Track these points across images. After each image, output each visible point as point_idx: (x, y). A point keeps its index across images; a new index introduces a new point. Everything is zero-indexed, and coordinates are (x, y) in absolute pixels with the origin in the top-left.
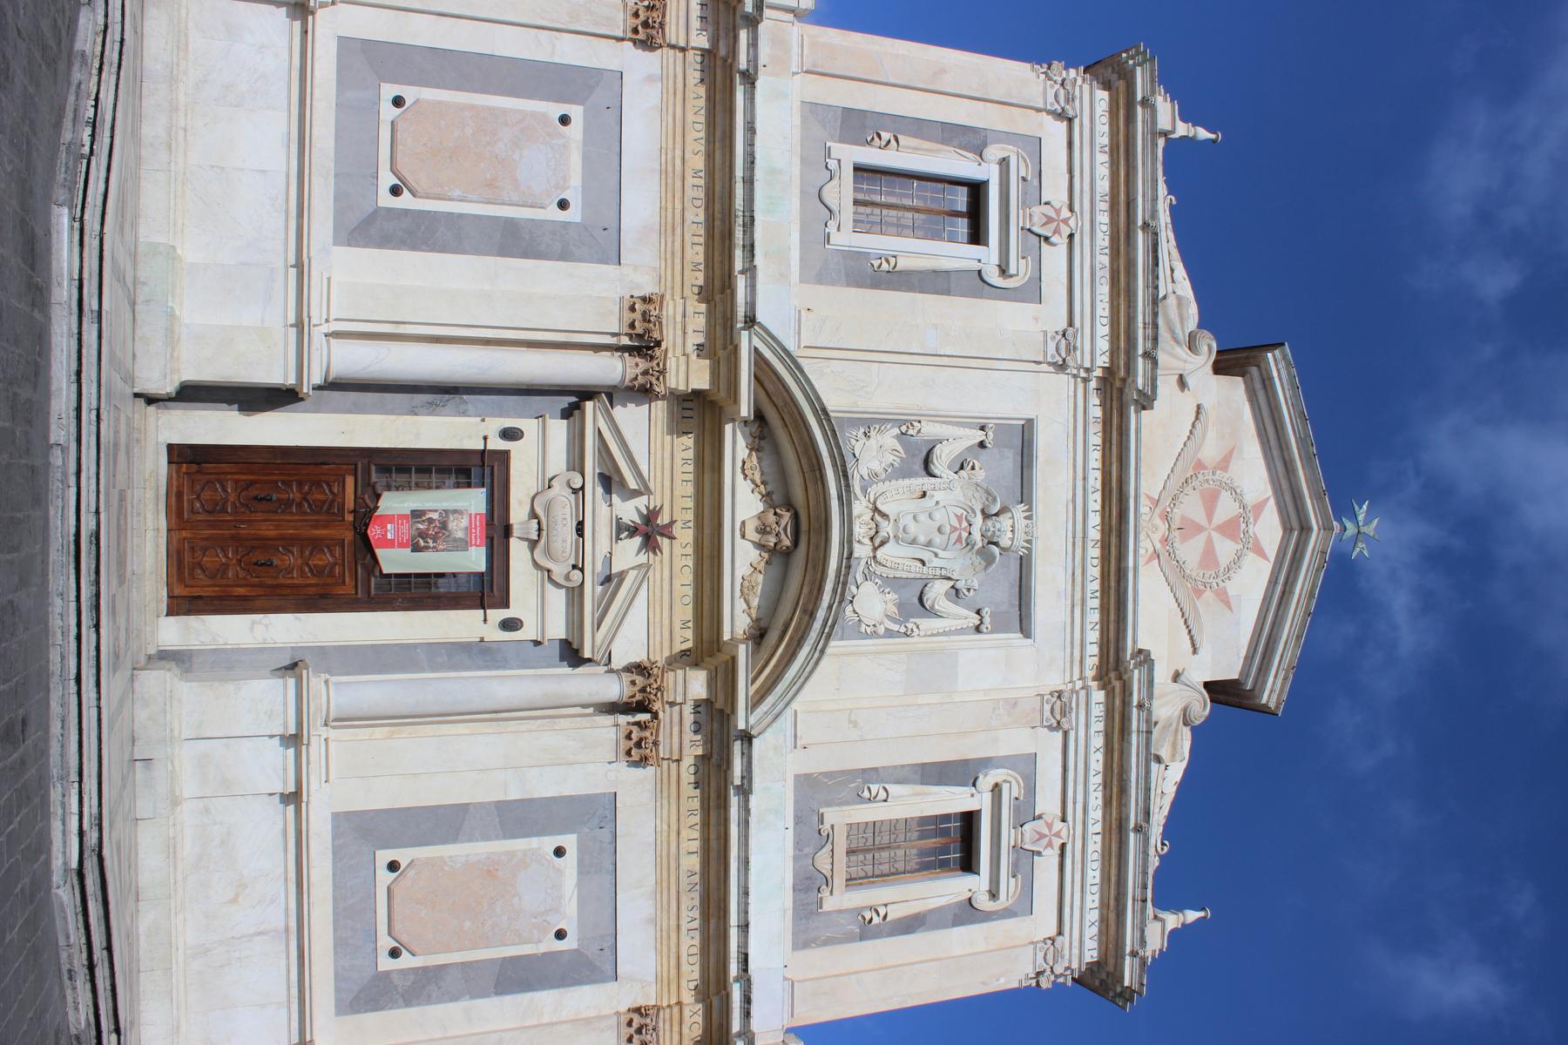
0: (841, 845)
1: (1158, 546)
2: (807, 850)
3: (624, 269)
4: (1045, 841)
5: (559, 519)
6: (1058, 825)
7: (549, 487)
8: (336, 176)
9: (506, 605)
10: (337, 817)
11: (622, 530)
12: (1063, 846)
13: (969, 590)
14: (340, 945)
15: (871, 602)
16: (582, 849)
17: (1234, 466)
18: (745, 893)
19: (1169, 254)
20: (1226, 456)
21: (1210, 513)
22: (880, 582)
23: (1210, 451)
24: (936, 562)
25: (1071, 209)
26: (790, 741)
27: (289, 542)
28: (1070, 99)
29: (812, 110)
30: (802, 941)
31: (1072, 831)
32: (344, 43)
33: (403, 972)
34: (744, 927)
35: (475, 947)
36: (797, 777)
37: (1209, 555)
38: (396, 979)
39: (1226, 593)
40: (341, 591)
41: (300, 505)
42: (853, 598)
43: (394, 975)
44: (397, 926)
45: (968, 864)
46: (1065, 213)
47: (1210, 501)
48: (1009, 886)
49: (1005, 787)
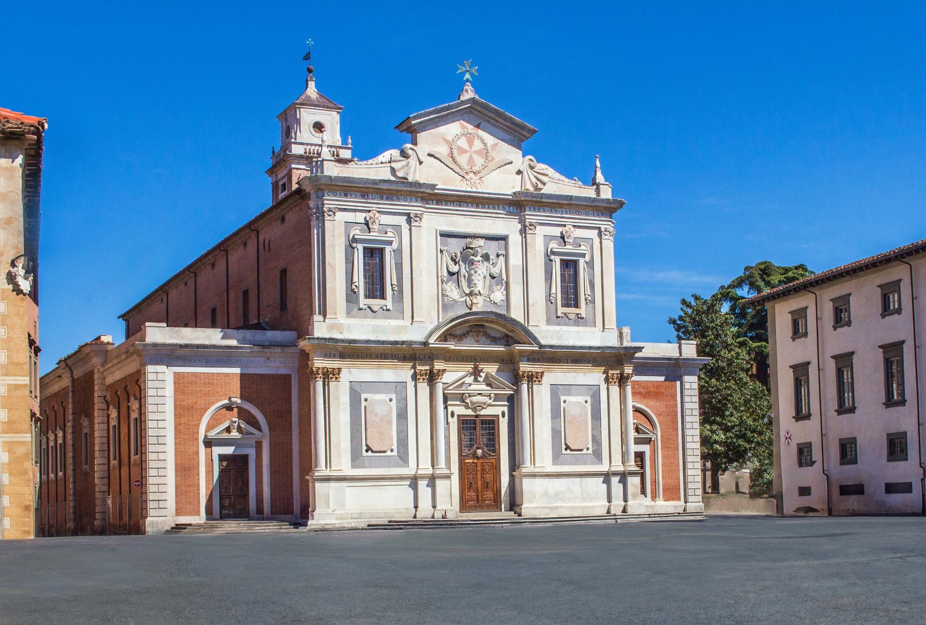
0: (566, 310)
1: (478, 177)
2: (567, 322)
3: (407, 381)
4: (571, 234)
5: (477, 400)
6: (567, 228)
7: (468, 403)
8: (389, 467)
9: (498, 415)
10: (553, 465)
11: (476, 380)
12: (574, 226)
13: (493, 259)
14: (585, 463)
15: (498, 295)
16: (564, 395)
17: (450, 138)
18: (581, 348)
19: (376, 164)
20: (446, 142)
21: (466, 152)
22: (490, 292)
23: (442, 150)
24: (485, 272)
25: (369, 211)
26: (538, 328)
27: (482, 477)
28: (330, 210)
29: (349, 313)
30: (594, 324)
31: (569, 223)
32: (353, 467)
33: (593, 446)
34: (590, 348)
35: (587, 427)
36: (547, 324)
37: (478, 152)
38: (594, 449)
39: (492, 145)
40: (495, 463)
41: (473, 475)
42: (494, 302)
43: (594, 449)
44: (582, 448)
45: (575, 263)
46: (371, 214)
47: (462, 151)
48: (584, 249)
49: (554, 250)
